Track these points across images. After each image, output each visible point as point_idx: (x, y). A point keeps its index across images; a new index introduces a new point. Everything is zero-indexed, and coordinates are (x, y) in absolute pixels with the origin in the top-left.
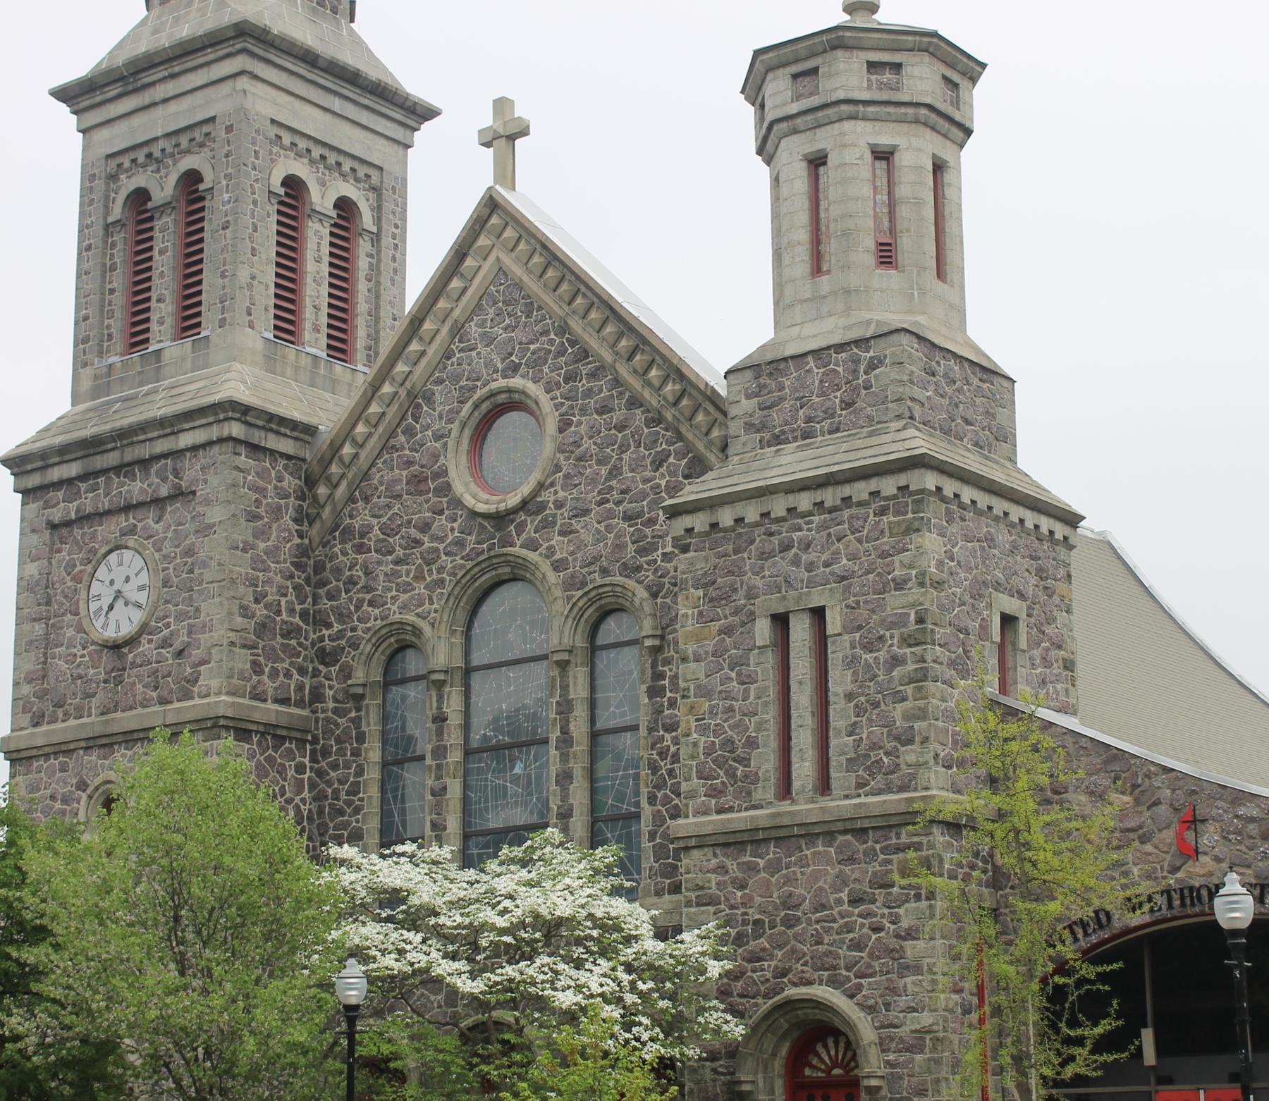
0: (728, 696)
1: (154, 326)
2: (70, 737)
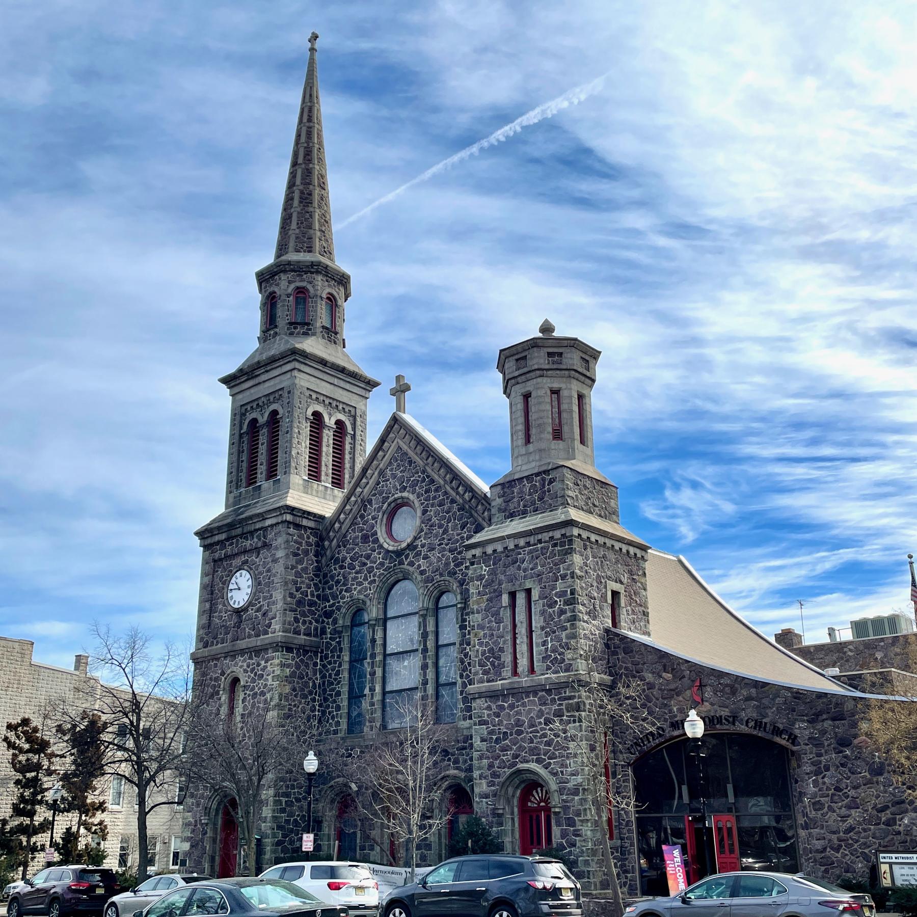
0: (491, 629)
1: (259, 476)
2: (218, 652)
